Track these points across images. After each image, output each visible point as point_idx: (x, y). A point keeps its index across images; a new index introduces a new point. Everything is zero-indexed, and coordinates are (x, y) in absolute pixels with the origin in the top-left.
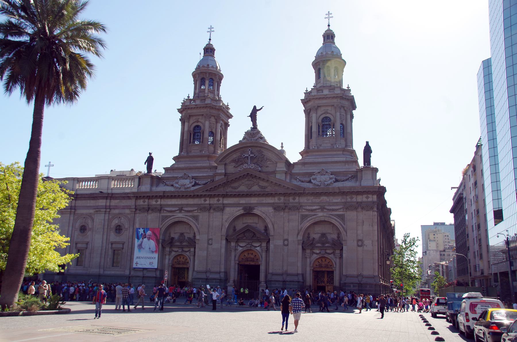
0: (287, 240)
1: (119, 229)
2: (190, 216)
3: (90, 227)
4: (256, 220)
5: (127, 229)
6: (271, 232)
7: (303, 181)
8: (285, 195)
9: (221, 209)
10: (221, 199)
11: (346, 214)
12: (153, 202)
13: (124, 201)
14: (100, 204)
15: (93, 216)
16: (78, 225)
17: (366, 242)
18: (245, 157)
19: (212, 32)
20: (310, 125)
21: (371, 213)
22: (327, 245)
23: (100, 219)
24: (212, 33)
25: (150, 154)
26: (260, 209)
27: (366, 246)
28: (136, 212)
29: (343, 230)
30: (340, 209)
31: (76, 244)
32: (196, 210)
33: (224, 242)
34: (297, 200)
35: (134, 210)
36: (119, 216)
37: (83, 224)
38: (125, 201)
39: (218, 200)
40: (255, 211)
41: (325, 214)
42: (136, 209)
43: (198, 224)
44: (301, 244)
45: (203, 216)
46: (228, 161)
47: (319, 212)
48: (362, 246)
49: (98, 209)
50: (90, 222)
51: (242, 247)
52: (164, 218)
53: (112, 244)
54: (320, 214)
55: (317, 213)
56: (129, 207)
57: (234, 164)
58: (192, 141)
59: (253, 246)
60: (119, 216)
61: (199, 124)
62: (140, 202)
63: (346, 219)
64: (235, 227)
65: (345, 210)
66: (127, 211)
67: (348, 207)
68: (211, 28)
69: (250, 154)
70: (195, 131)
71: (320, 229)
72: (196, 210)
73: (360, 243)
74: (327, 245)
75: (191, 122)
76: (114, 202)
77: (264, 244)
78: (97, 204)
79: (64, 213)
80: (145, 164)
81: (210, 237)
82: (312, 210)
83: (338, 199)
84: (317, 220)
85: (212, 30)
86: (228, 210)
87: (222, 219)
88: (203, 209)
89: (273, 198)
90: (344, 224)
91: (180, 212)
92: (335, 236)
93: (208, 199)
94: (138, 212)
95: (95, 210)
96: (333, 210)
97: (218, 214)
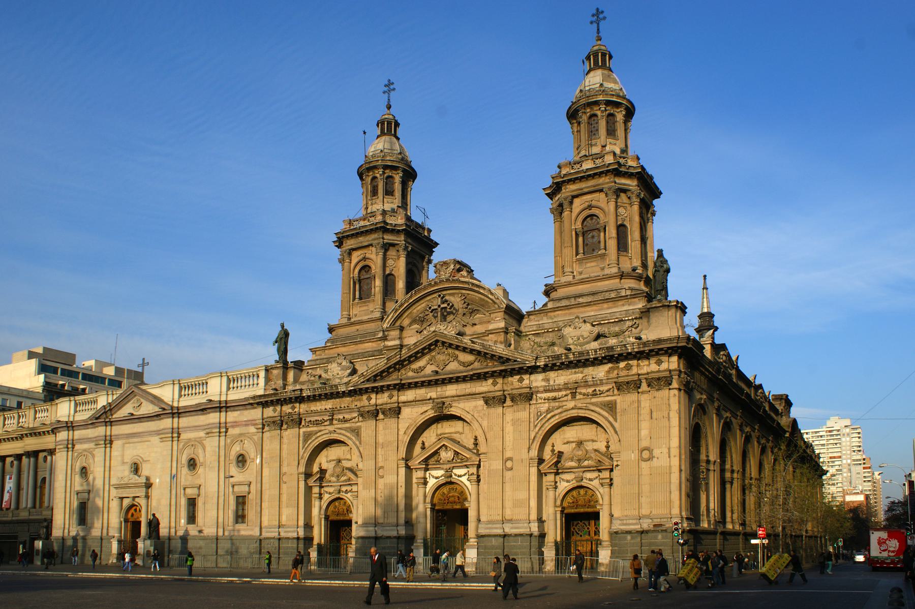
0: (510, 459)
1: (242, 460)
2: (346, 429)
3: (202, 460)
4: (458, 425)
5: (253, 459)
6: (482, 448)
7: (541, 344)
8: (504, 374)
9: (396, 412)
10: (395, 393)
11: (618, 401)
12: (287, 409)
13: (246, 412)
14: (212, 421)
15: (204, 442)
16: (184, 459)
17: (656, 452)
18: (433, 310)
21: (665, 393)
22: (586, 463)
23: (212, 444)
25: (283, 326)
26: (462, 405)
27: (658, 458)
28: (264, 431)
29: (612, 431)
30: (608, 391)
31: (184, 489)
32: (355, 418)
33: (402, 471)
34: (526, 382)
35: (261, 426)
36: (240, 438)
37: (192, 456)
38: (248, 411)
39: (391, 397)
40: (452, 409)
41: (580, 405)
42: (264, 425)
43: (360, 443)
44: (536, 465)
45: (367, 427)
46: (406, 322)
47: (567, 401)
48: (649, 460)
49: (208, 430)
50: (200, 451)
52: (308, 436)
53: (233, 486)
54: (571, 404)
55: (564, 403)
56: (251, 423)
57: (418, 326)
58: (357, 296)
60: (240, 438)
61: (367, 263)
62: (269, 412)
63: (618, 411)
64: (423, 443)
65: (616, 392)
66: (252, 429)
67: (621, 387)
69: (439, 303)
70: (362, 277)
71: (572, 433)
72: (355, 418)
73: (646, 454)
74: (586, 463)
75: (354, 261)
76: (232, 416)
78: (208, 422)
79: (164, 439)
80: (274, 345)
81: (380, 464)
82: (555, 399)
83: (600, 372)
84: (565, 416)
86: (406, 412)
87: (398, 430)
88: (365, 414)
89: (484, 383)
90: (616, 420)
91: (331, 424)
92: (602, 446)
93: (373, 396)
94: (266, 428)
95: (205, 432)
97: (391, 422)
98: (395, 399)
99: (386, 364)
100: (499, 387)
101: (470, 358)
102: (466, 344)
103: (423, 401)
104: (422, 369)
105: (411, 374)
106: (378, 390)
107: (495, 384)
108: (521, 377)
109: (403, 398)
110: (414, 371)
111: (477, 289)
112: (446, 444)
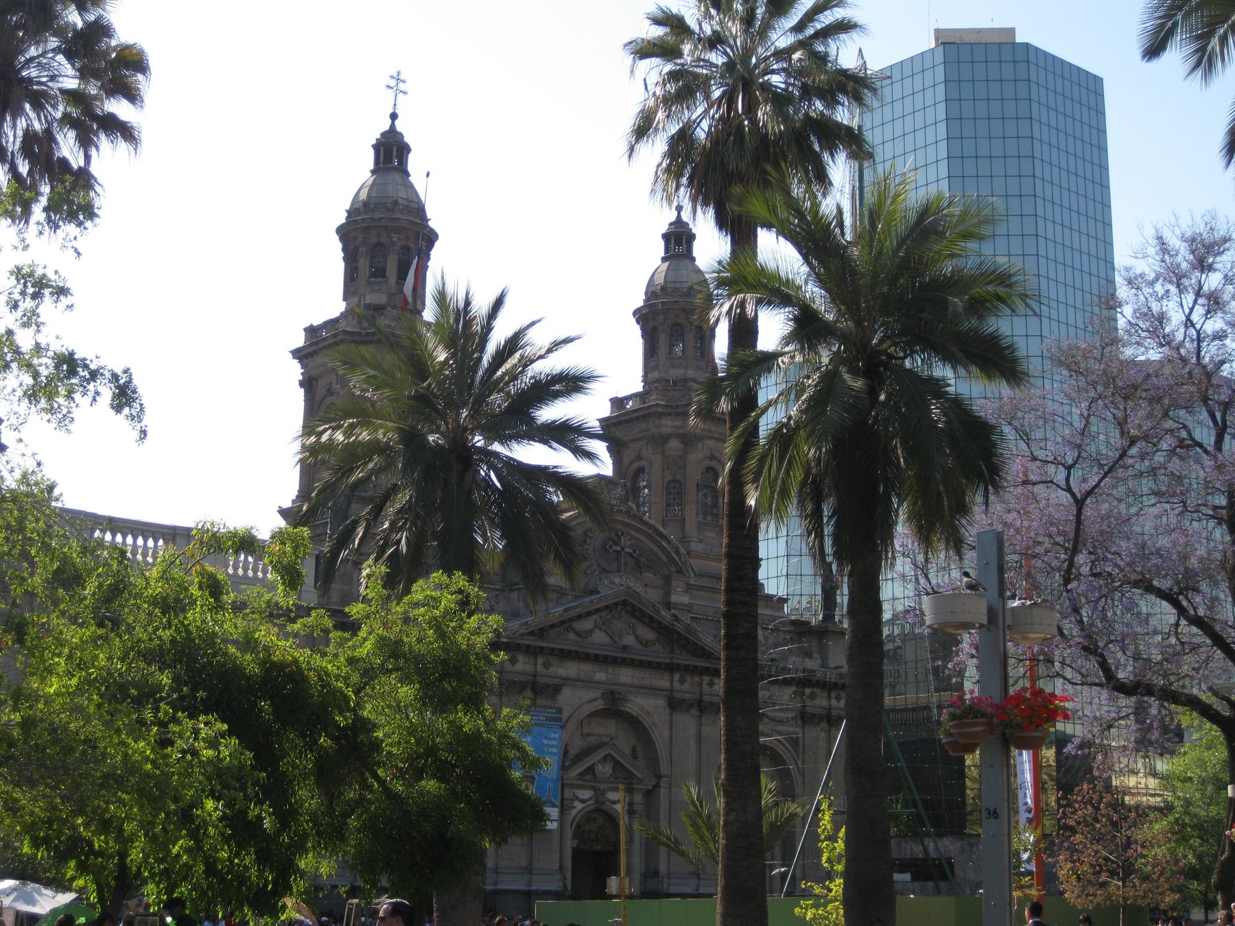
6: (664, 769)
10: (554, 661)
19: (401, 94)
20: (668, 478)
24: (400, 96)
26: (640, 700)
39: (547, 665)
40: (629, 705)
51: (583, 801)
59: (609, 801)
63: (801, 746)
65: (799, 722)
67: (805, 718)
68: (398, 78)
77: (638, 798)
85: (402, 86)
93: (521, 658)
96: (781, 722)
98: (552, 670)
99: (561, 615)
100: (686, 686)
101: (648, 634)
102: (663, 617)
103: (589, 683)
104: (589, 632)
105: (572, 636)
106: (532, 652)
107: (682, 681)
108: (711, 680)
109: (562, 672)
110: (577, 634)
111: (659, 539)
112: (612, 753)
